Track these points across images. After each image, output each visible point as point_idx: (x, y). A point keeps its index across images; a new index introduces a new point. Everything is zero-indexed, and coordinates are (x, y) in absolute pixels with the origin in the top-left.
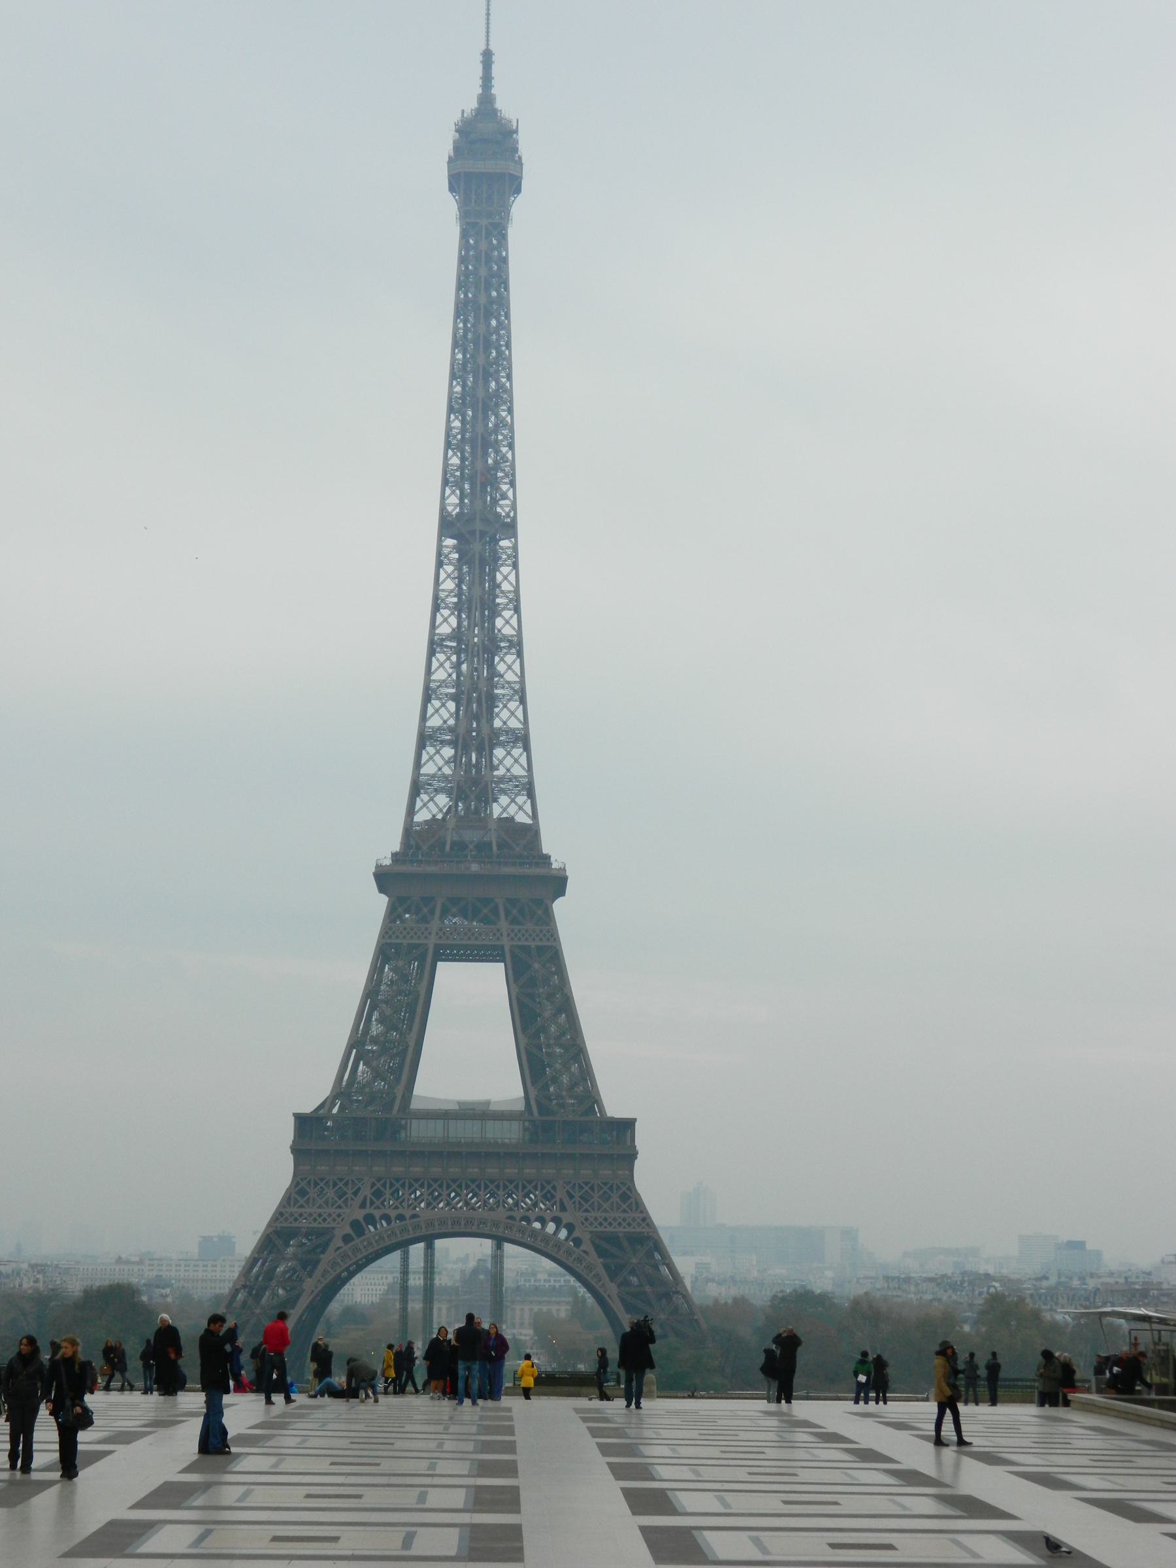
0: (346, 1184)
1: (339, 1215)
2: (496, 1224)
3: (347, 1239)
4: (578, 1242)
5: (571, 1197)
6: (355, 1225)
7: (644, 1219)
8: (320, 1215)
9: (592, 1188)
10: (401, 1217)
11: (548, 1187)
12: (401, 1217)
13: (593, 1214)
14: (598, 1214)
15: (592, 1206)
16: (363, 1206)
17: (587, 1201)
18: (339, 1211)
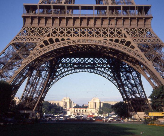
0: (43, 29)
1: (39, 39)
2: (99, 42)
3: (42, 46)
4: (133, 47)
5: (128, 33)
6: (46, 43)
7: (158, 40)
8: (32, 39)
9: (136, 30)
10: (63, 40)
11: (119, 30)
12: (63, 40)
13: (138, 38)
14: (140, 38)
15: (137, 35)
16: (49, 36)
17: (134, 34)
18: (40, 37)
